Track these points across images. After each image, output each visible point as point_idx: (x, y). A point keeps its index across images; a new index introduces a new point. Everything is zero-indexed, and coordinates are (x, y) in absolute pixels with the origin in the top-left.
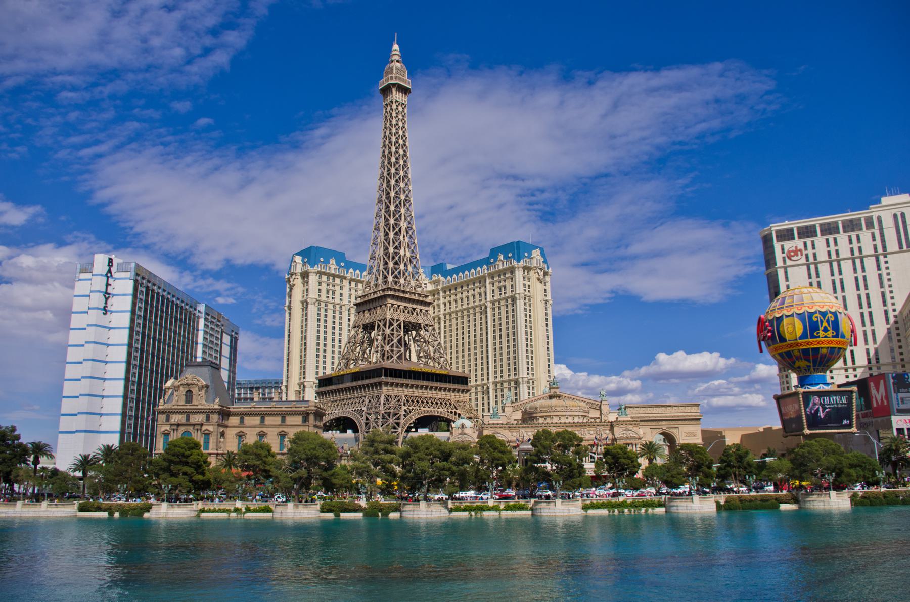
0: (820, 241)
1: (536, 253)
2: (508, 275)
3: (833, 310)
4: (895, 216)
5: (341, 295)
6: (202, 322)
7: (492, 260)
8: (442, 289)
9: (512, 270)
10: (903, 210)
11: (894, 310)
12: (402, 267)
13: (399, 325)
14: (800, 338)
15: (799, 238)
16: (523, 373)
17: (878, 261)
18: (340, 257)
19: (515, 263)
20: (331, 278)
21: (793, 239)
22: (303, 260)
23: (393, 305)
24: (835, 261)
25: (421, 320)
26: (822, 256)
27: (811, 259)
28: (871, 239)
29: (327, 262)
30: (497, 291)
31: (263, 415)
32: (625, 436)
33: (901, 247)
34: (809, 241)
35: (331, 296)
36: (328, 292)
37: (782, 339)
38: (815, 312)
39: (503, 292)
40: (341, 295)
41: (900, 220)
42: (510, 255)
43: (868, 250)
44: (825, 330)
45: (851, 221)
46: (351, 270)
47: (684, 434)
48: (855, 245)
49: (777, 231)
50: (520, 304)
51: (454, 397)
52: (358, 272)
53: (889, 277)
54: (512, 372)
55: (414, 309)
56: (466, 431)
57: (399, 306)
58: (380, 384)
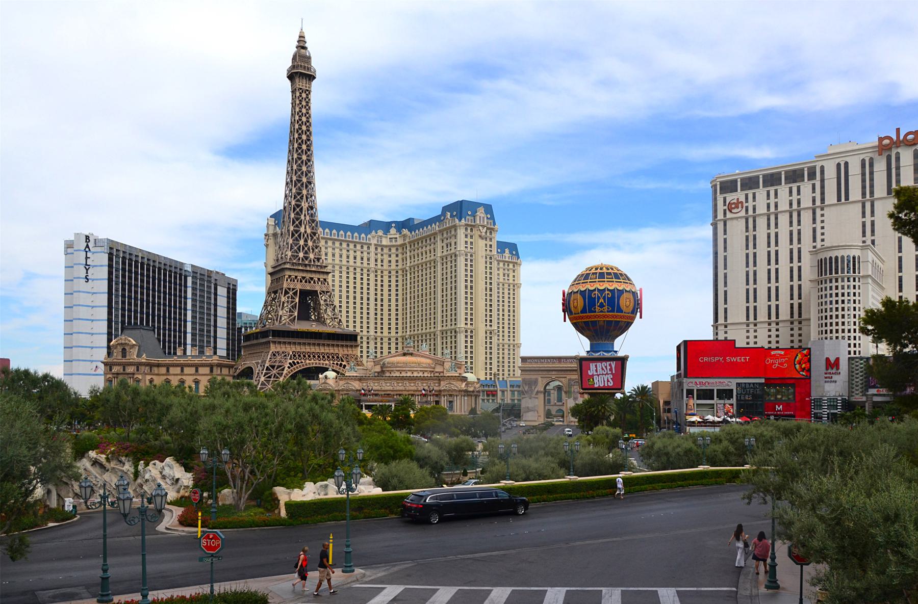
1: (481, 213)
6: (190, 280)
12: (302, 242)
13: (295, 294)
14: (582, 312)
16: (461, 324)
17: (814, 213)
23: (290, 276)
24: (772, 217)
25: (318, 288)
26: (762, 209)
27: (751, 212)
31: (182, 367)
33: (839, 199)
34: (750, 193)
42: (455, 213)
43: (806, 203)
44: (602, 306)
48: (795, 197)
51: (341, 352)
52: (327, 230)
53: (823, 231)
55: (312, 279)
56: (328, 381)
57: (296, 277)
58: (269, 342)
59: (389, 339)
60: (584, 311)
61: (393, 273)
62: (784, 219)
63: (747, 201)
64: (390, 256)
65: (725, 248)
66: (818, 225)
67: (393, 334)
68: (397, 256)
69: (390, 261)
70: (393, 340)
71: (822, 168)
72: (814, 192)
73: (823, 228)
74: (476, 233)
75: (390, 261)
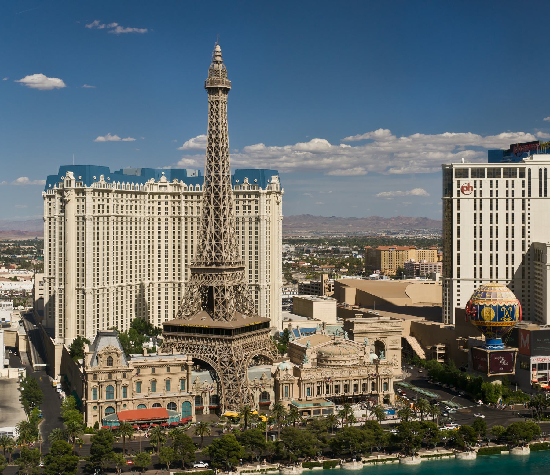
0: (486, 181)
2: (253, 197)
3: (512, 305)
4: (541, 170)
5: (108, 207)
7: (237, 181)
8: (184, 194)
9: (258, 194)
10: (546, 166)
11: (529, 241)
14: (492, 321)
15: (472, 177)
16: (263, 283)
18: (105, 170)
19: (261, 189)
20: (101, 193)
21: (467, 177)
24: (494, 200)
29: (98, 179)
30: (241, 209)
32: (385, 374)
33: (541, 195)
34: (478, 180)
37: (482, 319)
38: (503, 306)
39: (247, 210)
41: (543, 174)
43: (518, 194)
44: (507, 317)
45: (510, 169)
46: (114, 183)
47: (391, 342)
49: (456, 169)
54: (253, 279)
59: (159, 285)
60: (495, 319)
61: (163, 220)
62: (502, 204)
63: (475, 187)
64: (159, 203)
65: (459, 221)
66: (526, 212)
67: (163, 279)
68: (167, 203)
69: (159, 209)
70: (163, 285)
71: (530, 170)
72: (523, 187)
73: (529, 214)
75: (159, 209)
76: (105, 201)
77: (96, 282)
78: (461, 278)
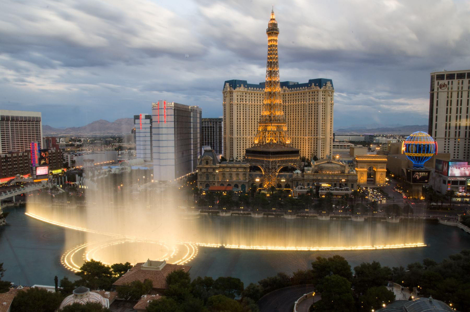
0: (455, 81)
1: (329, 84)
5: (246, 99)
15: (446, 79)
18: (244, 83)
19: (318, 88)
22: (230, 85)
28: (445, 120)
30: (311, 100)
34: (450, 81)
35: (242, 100)
36: (241, 99)
40: (246, 99)
46: (250, 88)
50: (320, 107)
54: (316, 134)
74: (327, 94)
76: (244, 97)
77: (239, 134)
78: (437, 137)
